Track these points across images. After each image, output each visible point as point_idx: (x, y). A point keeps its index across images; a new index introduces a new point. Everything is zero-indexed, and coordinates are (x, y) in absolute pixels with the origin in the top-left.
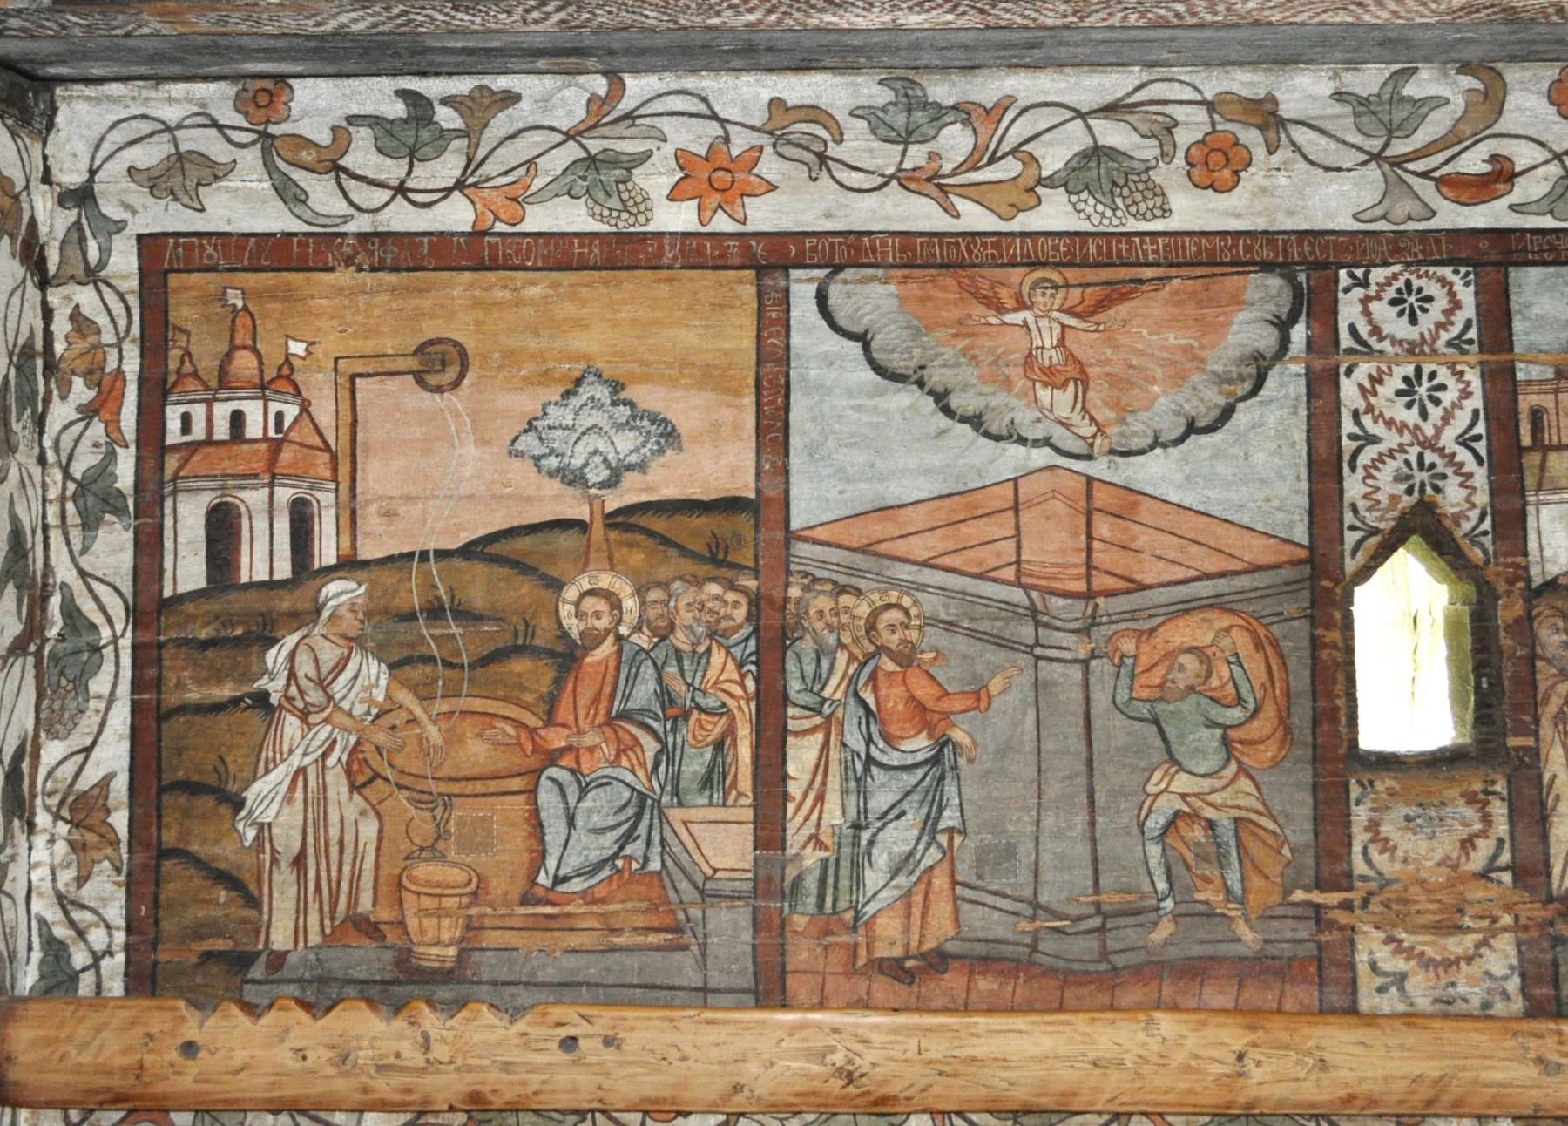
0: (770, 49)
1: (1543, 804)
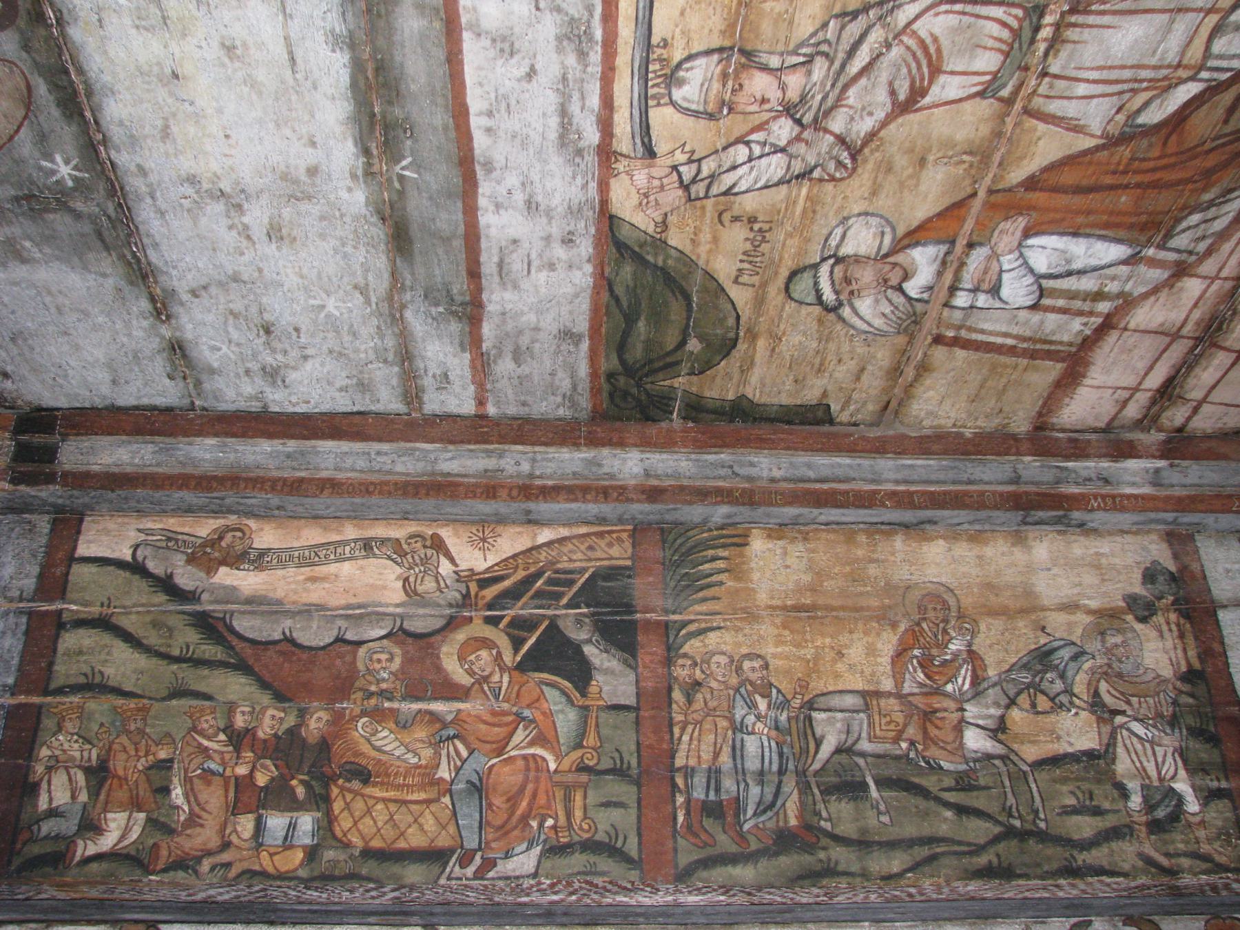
0: (565, 914)
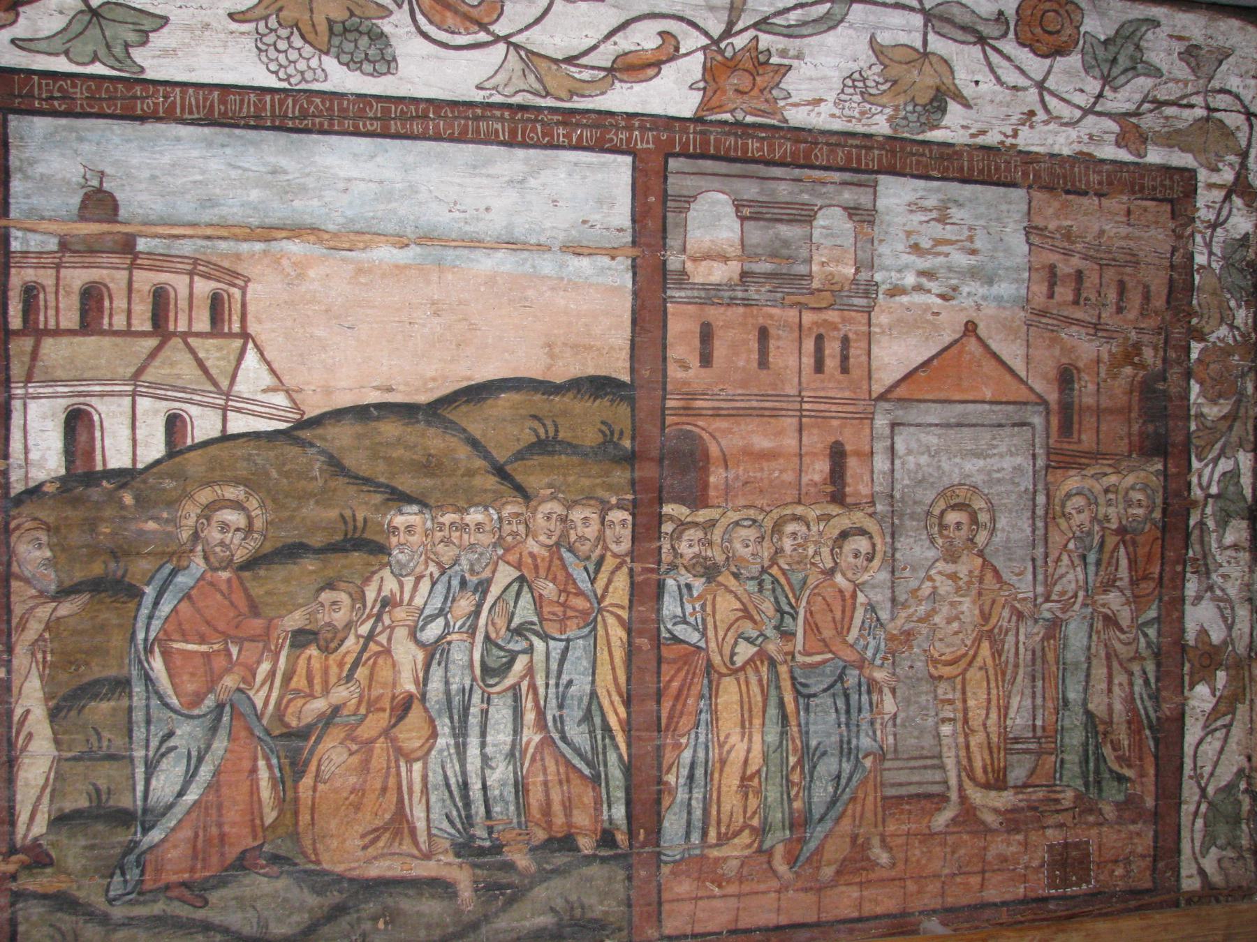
1: (11, 744)
